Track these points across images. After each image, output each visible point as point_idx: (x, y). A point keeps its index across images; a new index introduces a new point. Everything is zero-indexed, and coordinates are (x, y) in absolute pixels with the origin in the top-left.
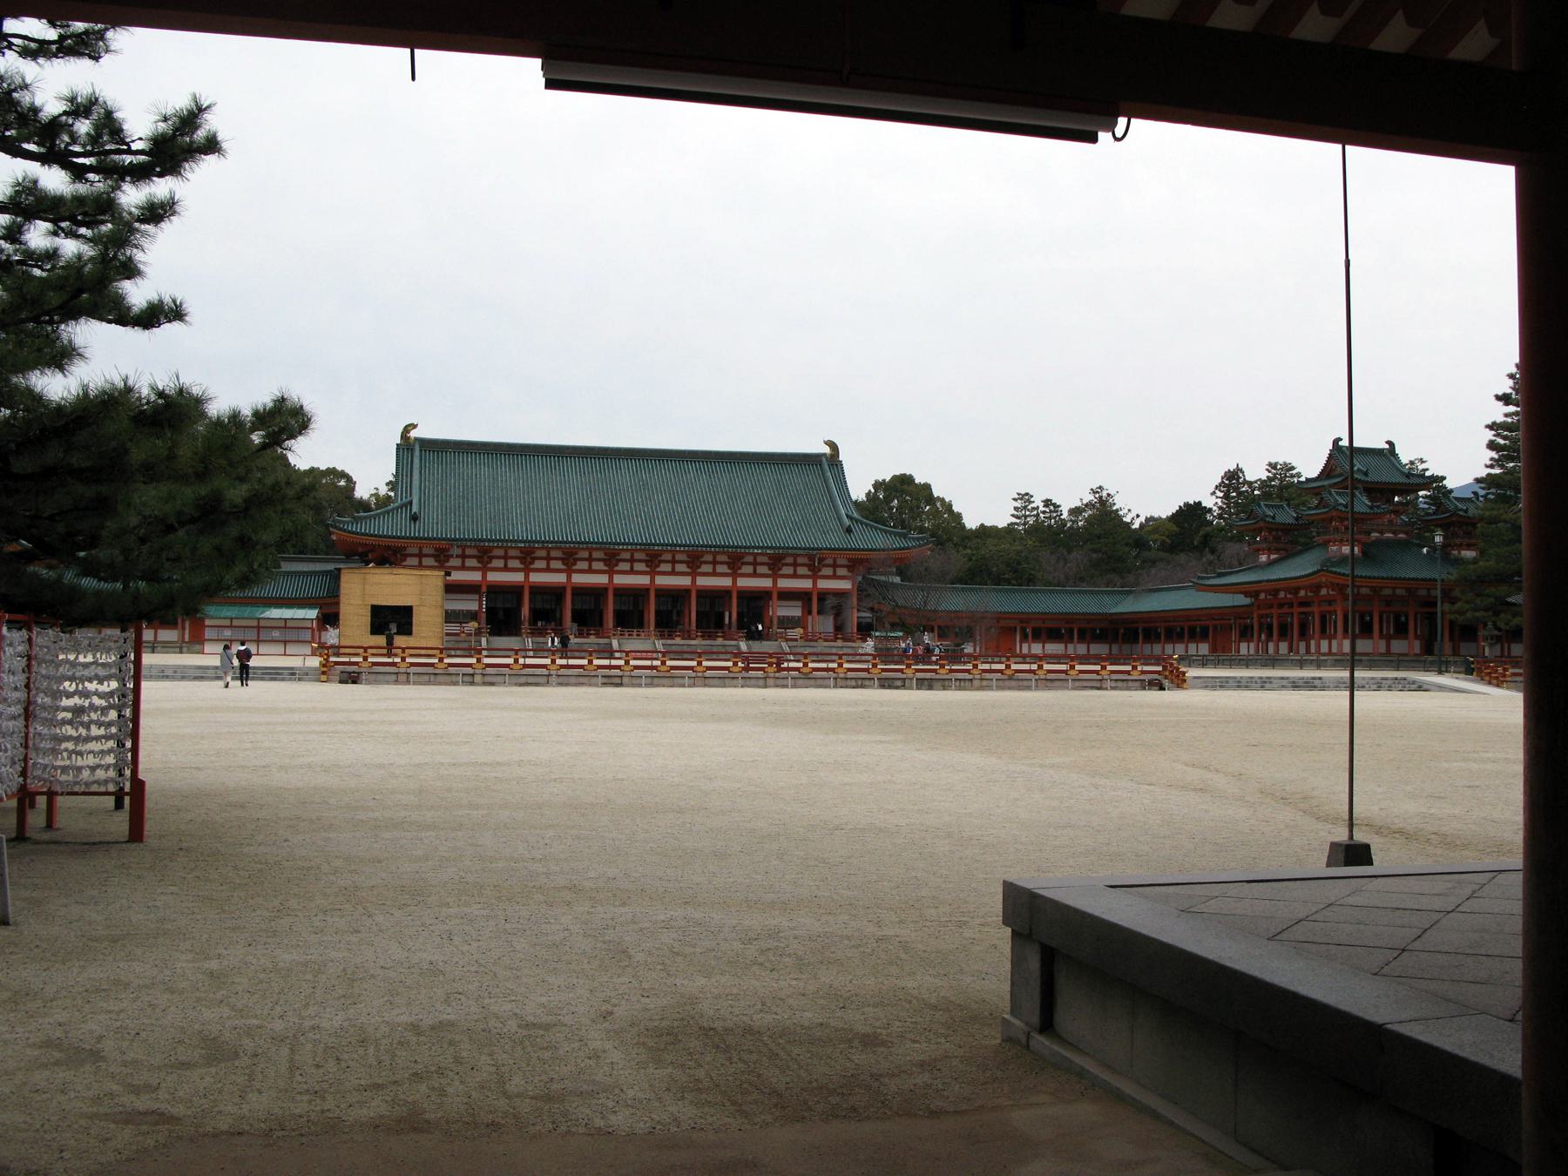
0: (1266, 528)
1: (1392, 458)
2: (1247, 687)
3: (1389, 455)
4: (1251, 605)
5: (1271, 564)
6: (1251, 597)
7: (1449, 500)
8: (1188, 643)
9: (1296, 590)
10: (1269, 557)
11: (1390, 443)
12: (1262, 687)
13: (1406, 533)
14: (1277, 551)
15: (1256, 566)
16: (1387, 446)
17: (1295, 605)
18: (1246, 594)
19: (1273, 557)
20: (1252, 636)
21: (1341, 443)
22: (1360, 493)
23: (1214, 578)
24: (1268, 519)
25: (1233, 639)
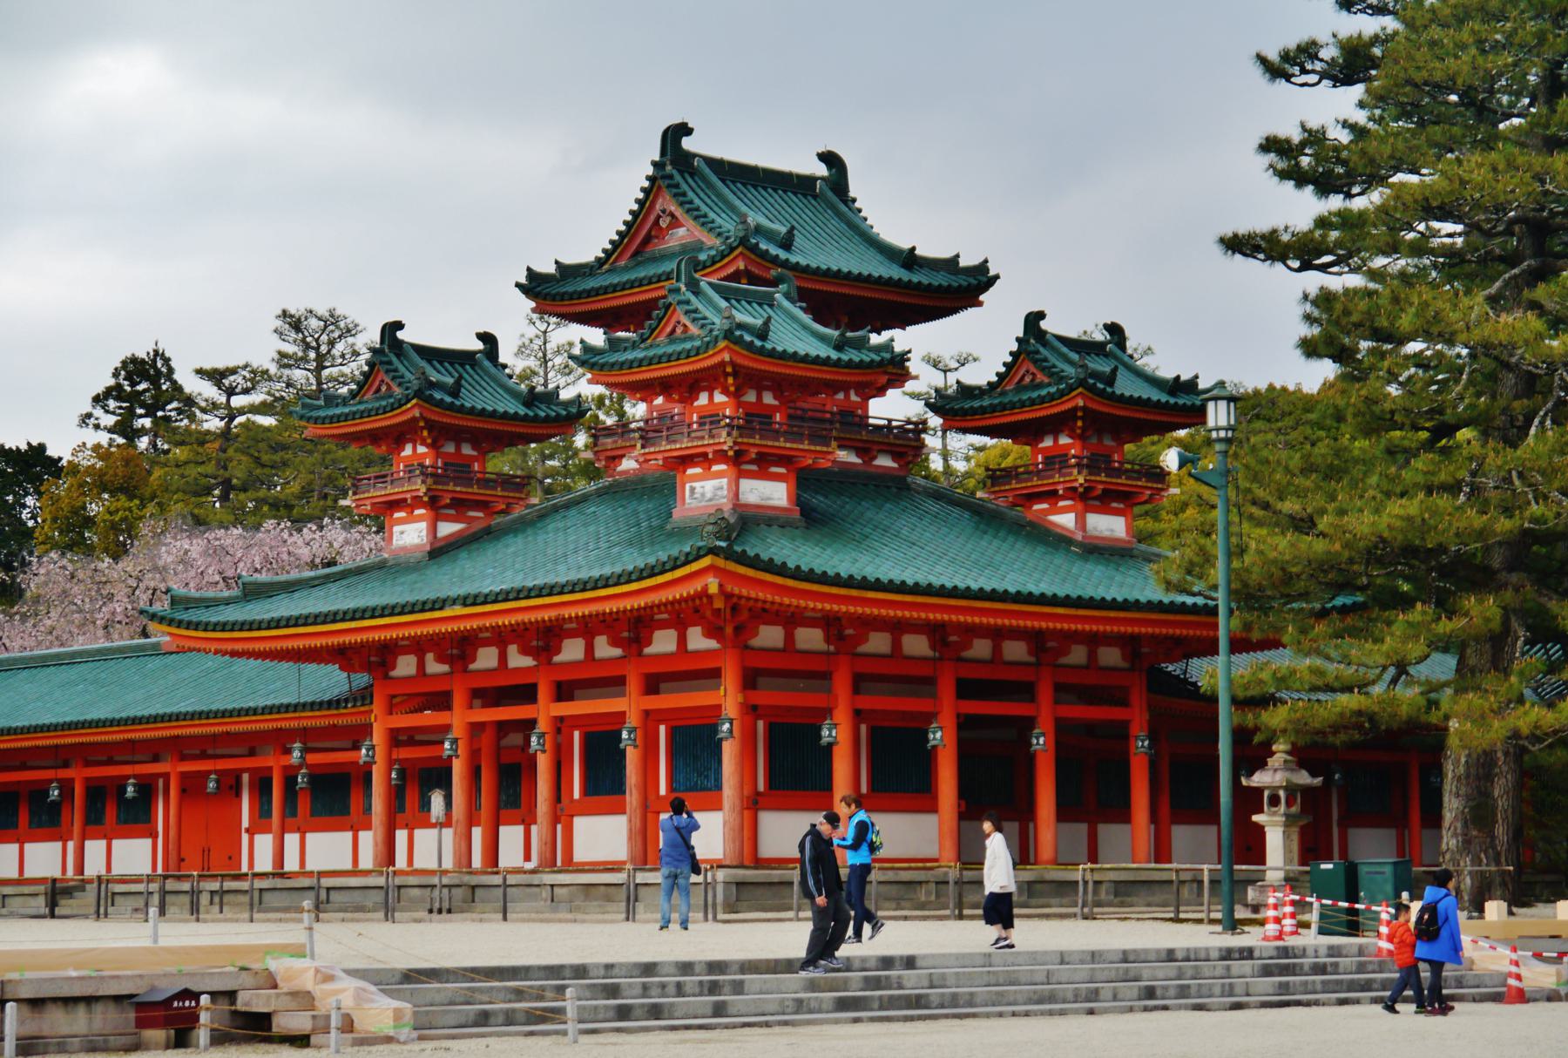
0: (431, 425)
1: (843, 208)
2: (656, 1012)
3: (830, 194)
4: (363, 696)
5: (439, 551)
6: (367, 667)
7: (1045, 344)
8: (83, 838)
9: (544, 638)
10: (433, 530)
11: (829, 158)
12: (719, 1010)
13: (896, 456)
14: (460, 506)
15: (381, 566)
16: (821, 170)
17: (543, 693)
18: (342, 656)
19: (447, 529)
20: (368, 809)
21: (687, 143)
22: (787, 296)
23: (227, 602)
24: (438, 395)
25: (245, 823)
